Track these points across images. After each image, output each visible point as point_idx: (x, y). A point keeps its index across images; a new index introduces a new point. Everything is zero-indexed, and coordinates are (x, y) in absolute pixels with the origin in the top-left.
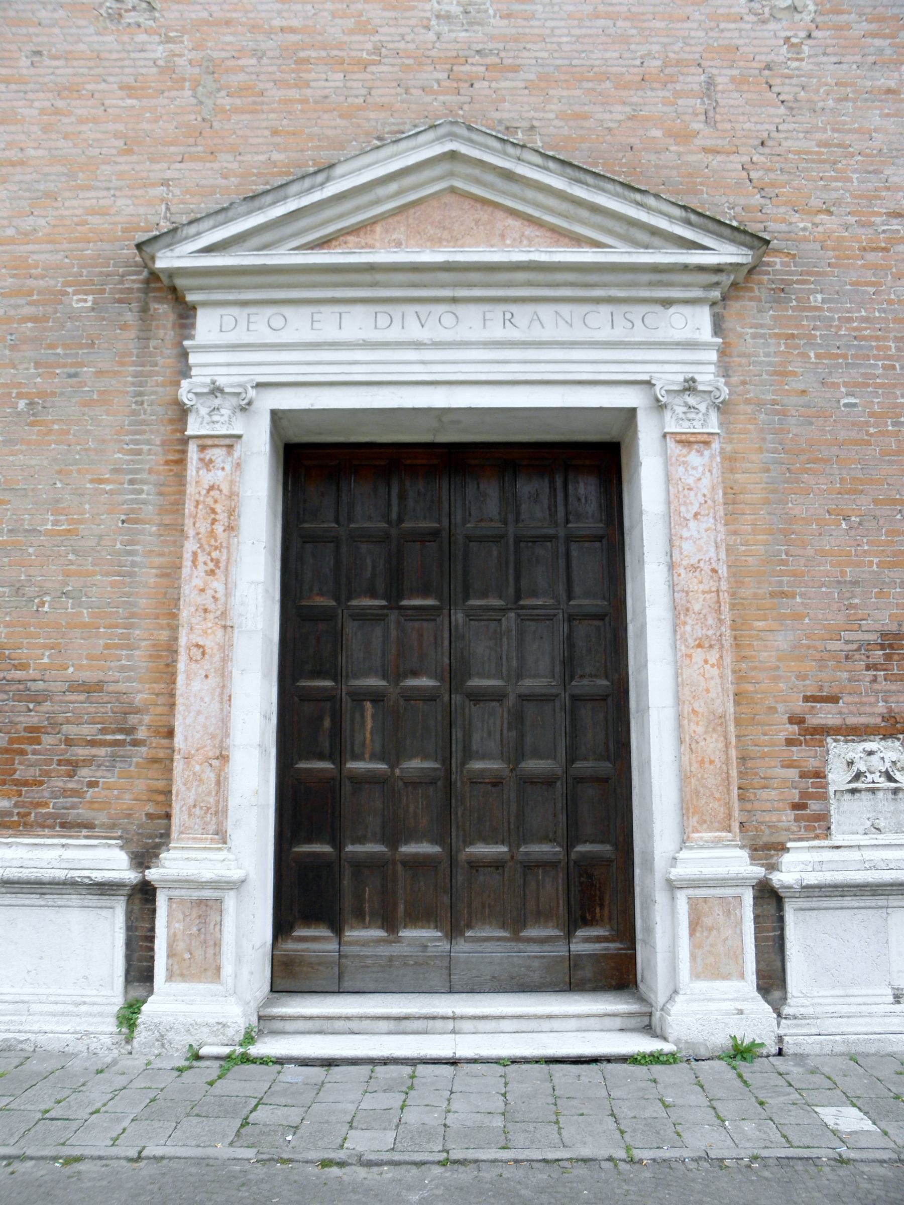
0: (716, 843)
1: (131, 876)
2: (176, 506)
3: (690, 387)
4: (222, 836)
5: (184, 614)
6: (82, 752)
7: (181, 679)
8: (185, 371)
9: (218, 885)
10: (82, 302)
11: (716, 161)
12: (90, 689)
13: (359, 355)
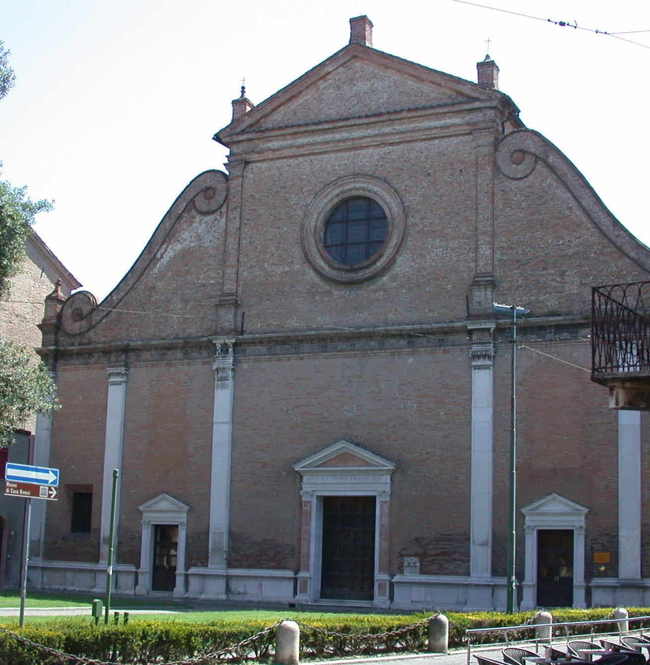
0: (384, 574)
1: (294, 576)
2: (301, 513)
3: (384, 492)
4: (308, 570)
5: (302, 532)
6: (287, 556)
7: (302, 543)
8: (301, 489)
9: (308, 578)
10: (284, 474)
11: (394, 443)
12: (288, 545)
13: (330, 486)
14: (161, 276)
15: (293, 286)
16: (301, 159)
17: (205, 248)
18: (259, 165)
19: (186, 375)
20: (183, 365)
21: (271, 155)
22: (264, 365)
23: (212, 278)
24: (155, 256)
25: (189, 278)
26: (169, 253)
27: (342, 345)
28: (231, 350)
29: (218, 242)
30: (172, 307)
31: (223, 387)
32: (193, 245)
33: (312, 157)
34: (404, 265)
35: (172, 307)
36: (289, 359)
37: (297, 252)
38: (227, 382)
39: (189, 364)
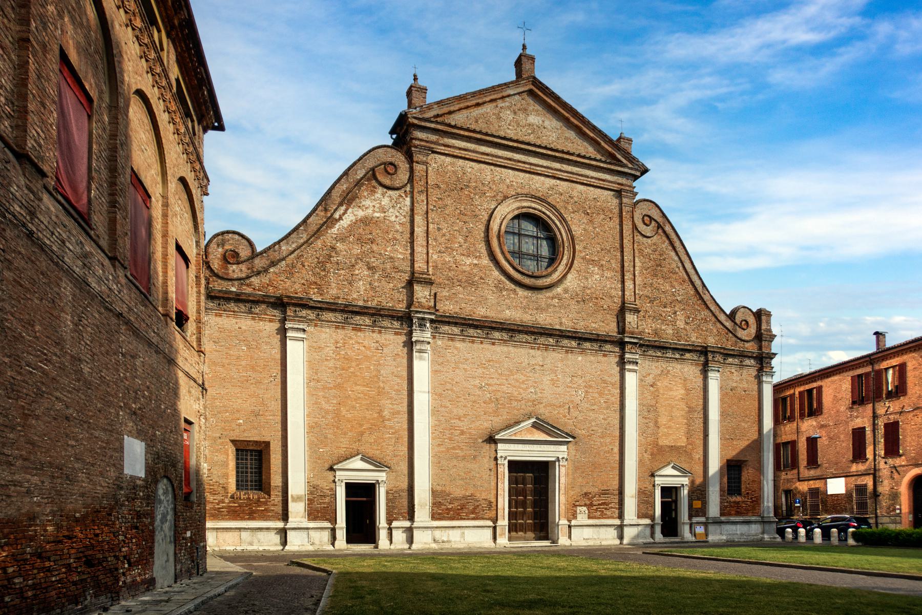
14: (342, 239)
15: (481, 278)
16: (483, 166)
17: (391, 222)
18: (443, 157)
19: (377, 342)
20: (373, 332)
21: (457, 152)
22: (458, 344)
23: (401, 253)
24: (332, 215)
25: (375, 247)
26: (349, 217)
27: (530, 338)
28: (428, 325)
29: (404, 220)
30: (357, 272)
31: (421, 358)
32: (377, 215)
33: (492, 167)
34: (572, 281)
35: (357, 272)
36: (482, 343)
37: (482, 247)
38: (426, 355)
39: (380, 332)
